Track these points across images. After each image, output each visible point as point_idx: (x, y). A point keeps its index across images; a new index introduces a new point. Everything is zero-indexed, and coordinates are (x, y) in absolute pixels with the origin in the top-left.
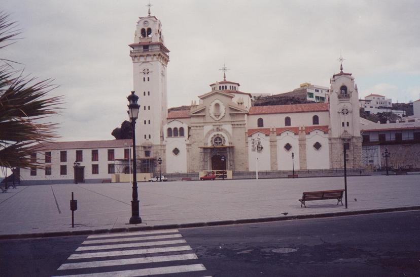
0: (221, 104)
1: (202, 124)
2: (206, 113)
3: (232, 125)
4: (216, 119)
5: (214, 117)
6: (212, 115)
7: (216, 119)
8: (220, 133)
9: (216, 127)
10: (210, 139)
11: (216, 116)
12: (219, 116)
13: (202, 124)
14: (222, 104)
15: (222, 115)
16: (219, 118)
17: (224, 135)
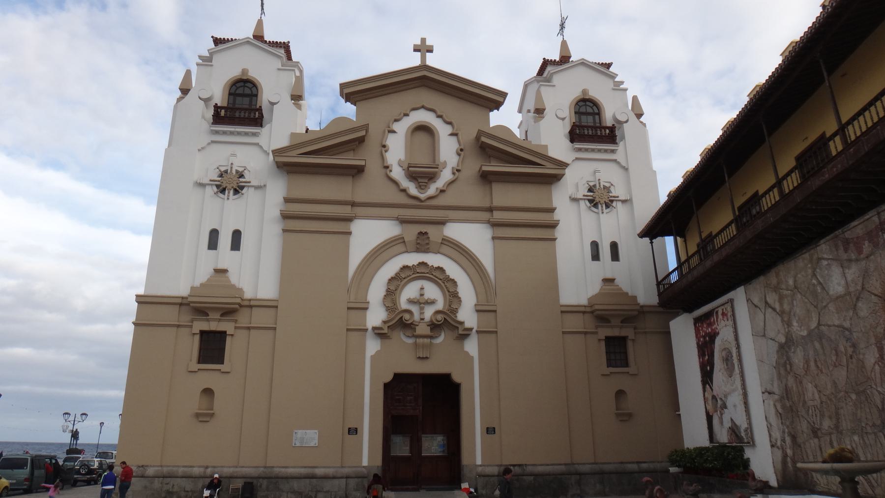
0: (443, 130)
1: (346, 210)
2: (366, 157)
3: (494, 225)
4: (413, 190)
5: (406, 183)
6: (397, 173)
7: (413, 190)
8: (434, 260)
9: (416, 229)
10: (376, 291)
11: (413, 176)
12: (432, 177)
13: (346, 210)
14: (448, 129)
15: (446, 176)
16: (432, 190)
17: (453, 270)
